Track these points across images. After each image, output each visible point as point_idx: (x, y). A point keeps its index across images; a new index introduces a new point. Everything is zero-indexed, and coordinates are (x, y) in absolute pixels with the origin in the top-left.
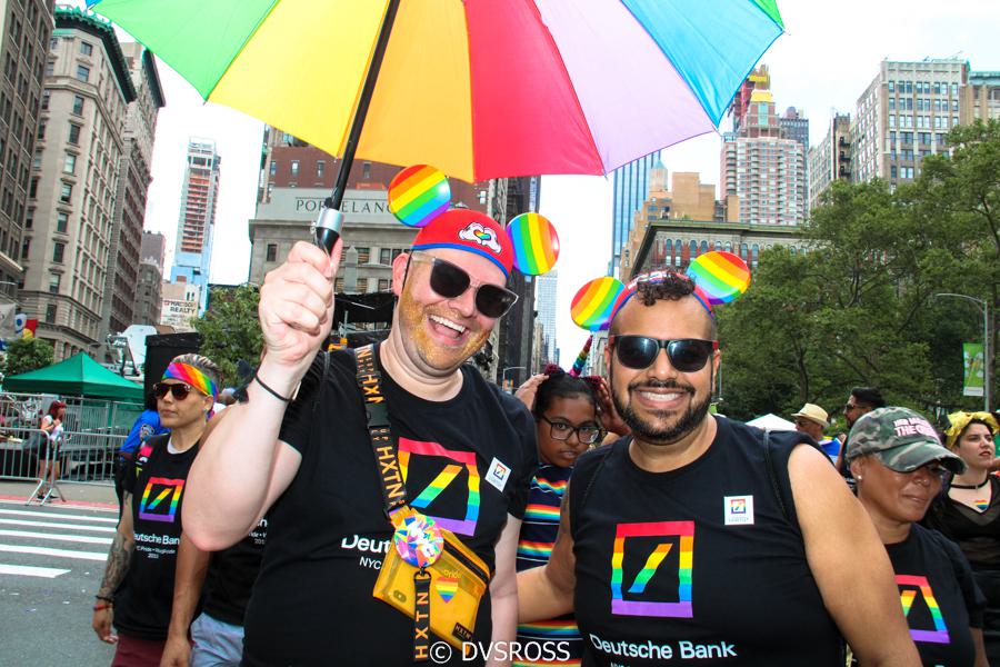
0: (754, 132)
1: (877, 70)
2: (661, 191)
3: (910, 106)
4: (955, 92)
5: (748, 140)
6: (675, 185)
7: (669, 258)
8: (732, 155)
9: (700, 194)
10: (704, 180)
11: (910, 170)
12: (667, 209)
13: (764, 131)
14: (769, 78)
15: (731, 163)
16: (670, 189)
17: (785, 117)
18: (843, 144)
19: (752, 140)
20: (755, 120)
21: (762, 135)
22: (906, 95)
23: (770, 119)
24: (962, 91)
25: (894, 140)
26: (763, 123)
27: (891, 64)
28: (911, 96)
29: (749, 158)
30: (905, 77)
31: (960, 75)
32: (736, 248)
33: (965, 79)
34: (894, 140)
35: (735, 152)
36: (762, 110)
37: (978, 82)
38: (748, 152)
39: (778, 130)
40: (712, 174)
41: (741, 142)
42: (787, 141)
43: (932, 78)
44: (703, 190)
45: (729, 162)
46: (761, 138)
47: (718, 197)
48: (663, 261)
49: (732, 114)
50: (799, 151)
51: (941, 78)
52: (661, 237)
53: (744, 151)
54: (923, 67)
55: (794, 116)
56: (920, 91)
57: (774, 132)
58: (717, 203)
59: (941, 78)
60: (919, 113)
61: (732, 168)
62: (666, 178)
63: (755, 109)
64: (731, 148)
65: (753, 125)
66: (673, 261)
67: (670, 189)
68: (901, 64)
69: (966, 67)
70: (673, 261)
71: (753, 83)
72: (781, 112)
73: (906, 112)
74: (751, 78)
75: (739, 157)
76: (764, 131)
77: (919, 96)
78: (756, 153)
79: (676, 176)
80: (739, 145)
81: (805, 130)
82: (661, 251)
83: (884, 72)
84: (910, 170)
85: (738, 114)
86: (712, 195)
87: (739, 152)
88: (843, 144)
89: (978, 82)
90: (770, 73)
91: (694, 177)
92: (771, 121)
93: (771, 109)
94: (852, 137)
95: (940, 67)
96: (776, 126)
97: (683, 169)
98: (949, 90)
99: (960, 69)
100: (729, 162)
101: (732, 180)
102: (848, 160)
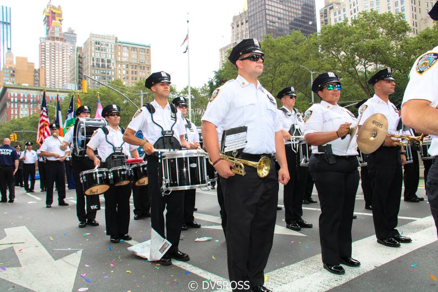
0: (53, 38)
1: (89, 36)
2: (10, 64)
3: (99, 50)
4: (113, 46)
5: (50, 41)
6: (17, 61)
7: (12, 99)
8: (43, 47)
9: (28, 66)
10: (30, 61)
11: (99, 71)
12: (14, 72)
13: (57, 38)
14: (61, 12)
15: (43, 50)
16: (15, 63)
17: (67, 32)
18: (79, 57)
19: (53, 42)
20: (53, 33)
21: (57, 40)
22: (98, 46)
23: (60, 34)
24: (115, 46)
25: (93, 61)
26: (57, 35)
27: (93, 34)
28: (99, 46)
29: (50, 49)
30: (98, 40)
31: (115, 40)
32: (38, 96)
33: (116, 42)
34: (93, 61)
35: (45, 46)
36: (57, 29)
37: (120, 44)
38: (50, 46)
39: (63, 39)
40: (35, 59)
41: (48, 42)
42: (67, 44)
43: (108, 41)
44: (29, 65)
45: (43, 49)
46: (56, 41)
47: (37, 67)
48: (10, 100)
49: (46, 25)
50: (71, 48)
51: (109, 41)
52: (8, 89)
53: (48, 46)
54: (104, 37)
55: (71, 32)
56: (102, 45)
57: (61, 39)
58: (35, 70)
59: (109, 41)
60: (102, 52)
61: (44, 52)
62: (13, 58)
63: (54, 29)
64: (43, 44)
65: (53, 36)
66: (14, 100)
67: (15, 63)
68: (96, 35)
69: (116, 39)
70: (14, 100)
71: (54, 13)
72: (65, 30)
73: (98, 51)
74: (54, 11)
75: (46, 48)
76: (57, 38)
77: (102, 46)
78: (53, 47)
79: (17, 58)
80: (46, 43)
81: (75, 38)
82: (9, 96)
83: (91, 37)
84: (99, 71)
85: (48, 26)
86: (34, 67)
87: (46, 46)
88: (79, 57)
89: (120, 44)
90: (63, 9)
91: (25, 59)
92: (60, 34)
93: (60, 30)
94: (83, 55)
95: (108, 37)
96: (62, 37)
97: (21, 56)
98: (111, 45)
99: (115, 39)
100: (43, 49)
101: (44, 55)
102: (81, 63)
